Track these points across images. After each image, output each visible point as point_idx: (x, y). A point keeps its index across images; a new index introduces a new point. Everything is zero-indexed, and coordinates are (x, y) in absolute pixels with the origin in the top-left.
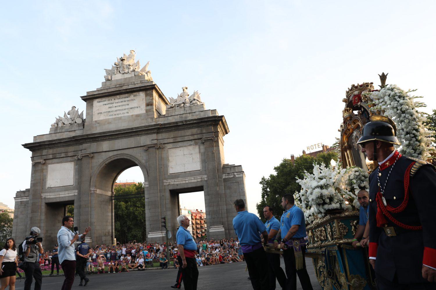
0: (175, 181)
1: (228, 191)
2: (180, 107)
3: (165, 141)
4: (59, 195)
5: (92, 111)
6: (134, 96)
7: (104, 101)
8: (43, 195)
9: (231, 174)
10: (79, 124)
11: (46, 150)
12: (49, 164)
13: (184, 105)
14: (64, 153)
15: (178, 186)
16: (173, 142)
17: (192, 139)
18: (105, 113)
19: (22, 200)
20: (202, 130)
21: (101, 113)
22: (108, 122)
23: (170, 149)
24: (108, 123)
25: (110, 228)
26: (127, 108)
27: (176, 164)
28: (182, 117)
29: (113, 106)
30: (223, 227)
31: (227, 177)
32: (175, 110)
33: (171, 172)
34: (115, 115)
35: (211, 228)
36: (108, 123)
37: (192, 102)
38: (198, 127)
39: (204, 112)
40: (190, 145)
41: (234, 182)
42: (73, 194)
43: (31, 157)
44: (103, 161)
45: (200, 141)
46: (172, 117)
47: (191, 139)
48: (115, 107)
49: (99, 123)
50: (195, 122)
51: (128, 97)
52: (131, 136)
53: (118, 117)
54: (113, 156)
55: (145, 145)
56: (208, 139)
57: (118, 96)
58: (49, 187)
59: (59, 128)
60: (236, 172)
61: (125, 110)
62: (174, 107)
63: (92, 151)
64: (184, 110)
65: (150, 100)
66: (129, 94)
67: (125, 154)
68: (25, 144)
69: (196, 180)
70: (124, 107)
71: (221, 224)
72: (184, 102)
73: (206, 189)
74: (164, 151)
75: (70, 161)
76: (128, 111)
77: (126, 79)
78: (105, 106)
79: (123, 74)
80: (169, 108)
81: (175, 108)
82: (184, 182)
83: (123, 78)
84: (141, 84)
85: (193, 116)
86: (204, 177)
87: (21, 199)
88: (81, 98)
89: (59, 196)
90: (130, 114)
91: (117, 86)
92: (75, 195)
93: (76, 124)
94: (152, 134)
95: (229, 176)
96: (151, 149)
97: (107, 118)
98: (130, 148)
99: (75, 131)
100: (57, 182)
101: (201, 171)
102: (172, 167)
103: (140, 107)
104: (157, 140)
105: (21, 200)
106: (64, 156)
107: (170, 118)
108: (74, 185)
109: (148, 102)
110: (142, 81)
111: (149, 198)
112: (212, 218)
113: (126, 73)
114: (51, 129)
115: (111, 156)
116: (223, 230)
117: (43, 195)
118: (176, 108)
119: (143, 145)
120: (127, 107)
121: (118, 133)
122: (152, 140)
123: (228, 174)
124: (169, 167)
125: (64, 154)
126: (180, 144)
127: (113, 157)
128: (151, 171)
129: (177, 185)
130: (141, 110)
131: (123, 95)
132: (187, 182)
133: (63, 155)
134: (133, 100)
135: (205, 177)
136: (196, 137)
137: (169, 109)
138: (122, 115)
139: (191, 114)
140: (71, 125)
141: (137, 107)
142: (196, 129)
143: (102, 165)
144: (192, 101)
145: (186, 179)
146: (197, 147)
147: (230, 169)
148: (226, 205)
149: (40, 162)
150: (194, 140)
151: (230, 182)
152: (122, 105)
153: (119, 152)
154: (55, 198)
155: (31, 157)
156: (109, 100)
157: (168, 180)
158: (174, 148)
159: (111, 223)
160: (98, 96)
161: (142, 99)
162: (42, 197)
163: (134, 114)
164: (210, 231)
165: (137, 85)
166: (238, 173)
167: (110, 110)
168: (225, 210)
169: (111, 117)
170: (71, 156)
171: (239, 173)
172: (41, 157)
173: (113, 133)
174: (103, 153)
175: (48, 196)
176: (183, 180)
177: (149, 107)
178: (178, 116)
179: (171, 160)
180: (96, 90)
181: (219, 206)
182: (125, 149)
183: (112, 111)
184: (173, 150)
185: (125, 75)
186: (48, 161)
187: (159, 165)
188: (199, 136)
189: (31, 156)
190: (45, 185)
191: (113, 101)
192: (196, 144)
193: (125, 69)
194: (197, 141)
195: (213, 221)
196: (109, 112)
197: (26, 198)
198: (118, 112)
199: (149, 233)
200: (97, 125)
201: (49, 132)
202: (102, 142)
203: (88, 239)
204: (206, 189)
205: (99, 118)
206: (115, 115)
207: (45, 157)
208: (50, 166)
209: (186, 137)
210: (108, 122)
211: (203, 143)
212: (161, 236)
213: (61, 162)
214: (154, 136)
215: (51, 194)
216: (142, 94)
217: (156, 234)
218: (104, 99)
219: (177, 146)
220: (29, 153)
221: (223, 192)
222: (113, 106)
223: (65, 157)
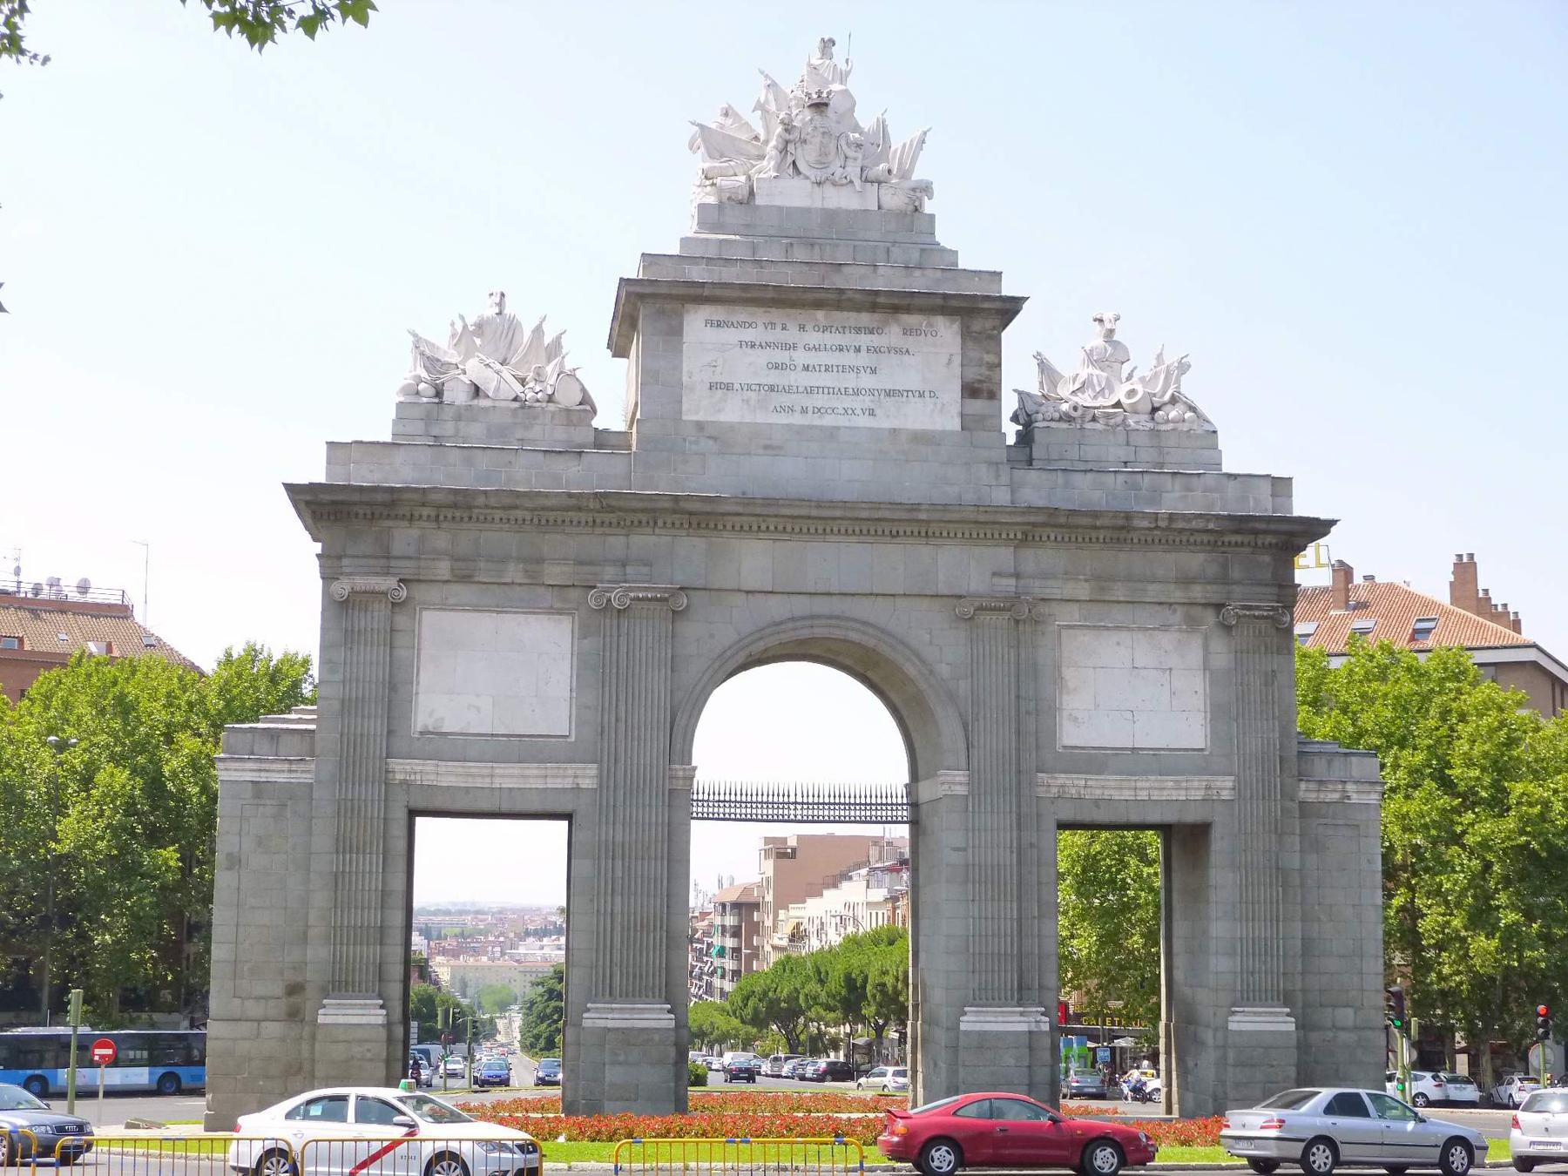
0: (1089, 783)
1: (1312, 859)
2: (1107, 425)
3: (1055, 591)
5: (678, 368)
6: (907, 331)
7: (742, 325)
8: (395, 764)
9: (1331, 787)
10: (568, 411)
11: (414, 533)
12: (428, 606)
14: (519, 560)
15: (1098, 806)
19: (263, 774)
20: (1225, 566)
21: (728, 387)
23: (1070, 631)
24: (766, 447)
26: (868, 386)
27: (1097, 706)
28: (1136, 487)
30: (1288, 1015)
31: (1311, 797)
33: (1068, 742)
35: (1234, 1013)
38: (1213, 546)
39: (1239, 479)
40: (1165, 627)
41: (1341, 822)
42: (568, 783)
44: (740, 641)
45: (1210, 617)
46: (1089, 475)
48: (806, 368)
49: (715, 438)
50: (1211, 526)
51: (871, 332)
53: (822, 428)
54: (793, 619)
55: (957, 591)
56: (1257, 613)
57: (820, 314)
58: (431, 729)
59: (448, 413)
60: (1356, 782)
61: (854, 397)
63: (681, 578)
64: (1128, 444)
65: (984, 371)
66: (877, 316)
67: (856, 620)
68: (311, 484)
69: (1183, 792)
70: (850, 381)
71: (1279, 999)
73: (1222, 838)
74: (1043, 634)
75: (551, 607)
77: (831, 217)
78: (749, 351)
79: (819, 184)
80: (1052, 420)
81: (1083, 422)
82: (1127, 795)
83: (818, 204)
84: (939, 274)
85: (1189, 489)
86: (1219, 784)
87: (260, 770)
89: (488, 780)
90: (883, 422)
91: (800, 254)
92: (577, 789)
93: (552, 407)
95: (1322, 796)
96: (986, 618)
97: (761, 418)
100: (478, 710)
101: (1207, 753)
102: (1076, 718)
103: (933, 394)
104: (1017, 576)
105: (257, 774)
107: (1083, 482)
109: (973, 374)
111: (965, 849)
112: (1242, 972)
113: (834, 184)
114: (400, 405)
115: (777, 619)
116: (1292, 1027)
117: (397, 768)
118: (1089, 426)
119: (943, 590)
120: (867, 381)
123: (1321, 782)
124: (1061, 717)
126: (1120, 614)
127: (790, 625)
128: (981, 721)
129: (1097, 802)
130: (941, 411)
132: (1143, 795)
133: (513, 572)
134: (898, 351)
135: (1225, 786)
136: (1197, 592)
137: (1053, 424)
138: (842, 421)
139: (1179, 481)
140: (522, 407)
142: (1202, 556)
143: (732, 656)
144: (1165, 404)
145: (1139, 784)
146: (1196, 642)
147: (1329, 763)
148: (1303, 921)
149: (385, 594)
150: (1185, 608)
153: (821, 606)
154: (467, 789)
155: (318, 555)
156: (773, 325)
157: (1056, 775)
158: (1089, 626)
160: (718, 292)
161: (945, 360)
162: (391, 776)
163: (902, 427)
164: (1232, 1026)
165: (917, 273)
166: (1361, 788)
167: (773, 378)
168: (1299, 943)
169: (783, 419)
171: (1367, 787)
172: (383, 562)
173: (814, 513)
174: (740, 599)
176: (1125, 784)
177: (977, 406)
178: (1121, 478)
179: (1071, 685)
180: (674, 249)
181: (1278, 921)
183: (787, 390)
184: (1085, 638)
185: (829, 190)
186: (420, 592)
187: (1018, 697)
188: (1214, 593)
190: (407, 717)
191: (792, 335)
192: (1192, 624)
193: (831, 158)
194: (1196, 611)
195: (1248, 985)
196: (772, 388)
197: (286, 766)
198: (819, 400)
199: (966, 1009)
201: (395, 423)
204: (1222, 838)
205: (719, 411)
206: (804, 411)
207: (407, 568)
208: (428, 617)
209: (1151, 587)
210: (768, 442)
211: (1227, 629)
212: (1024, 1028)
213: (499, 609)
214: (1004, 556)
215: (429, 766)
216: (947, 332)
217: (1000, 1019)
218: (741, 314)
219: (1101, 621)
221: (1297, 865)
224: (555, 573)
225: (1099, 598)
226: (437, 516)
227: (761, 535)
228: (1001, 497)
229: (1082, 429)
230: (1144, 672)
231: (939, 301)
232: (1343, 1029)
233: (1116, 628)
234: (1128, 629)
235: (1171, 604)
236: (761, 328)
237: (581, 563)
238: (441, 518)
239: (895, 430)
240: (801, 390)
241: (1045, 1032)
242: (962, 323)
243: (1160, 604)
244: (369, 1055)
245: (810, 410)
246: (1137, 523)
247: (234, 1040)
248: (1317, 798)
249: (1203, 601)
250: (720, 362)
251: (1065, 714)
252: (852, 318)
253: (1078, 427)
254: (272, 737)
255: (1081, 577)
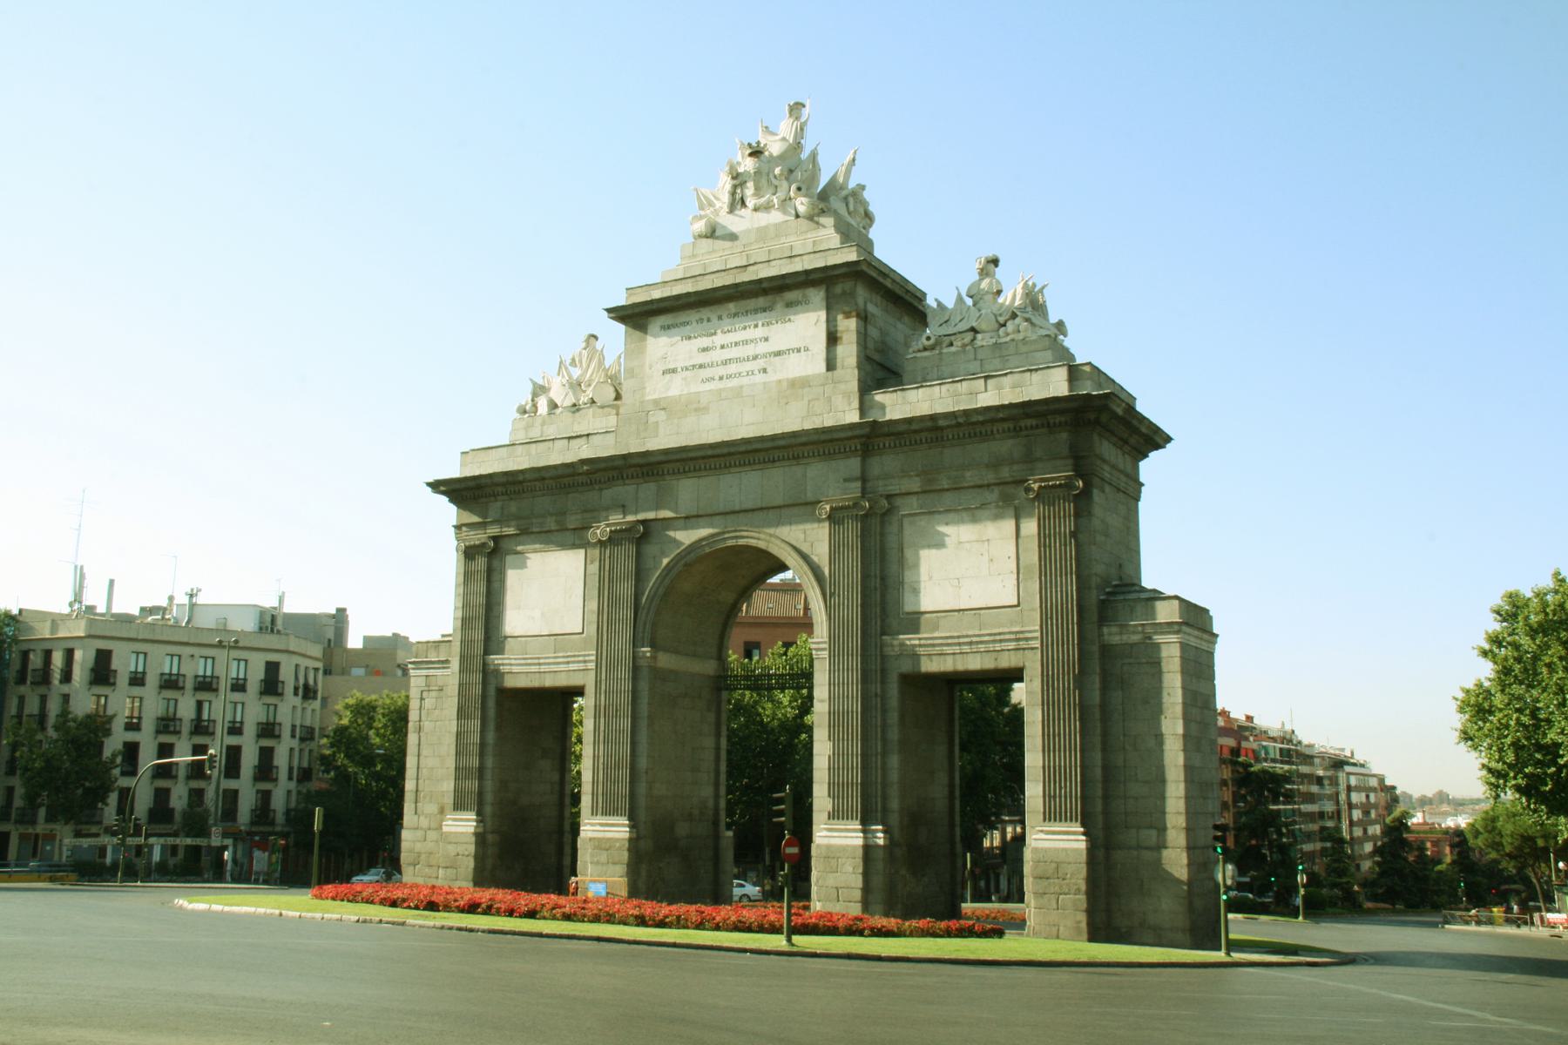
4: (539, 664)
11: (499, 504)
13: (974, 339)
14: (551, 515)
16: (919, 490)
17: (993, 481)
18: (687, 369)
21: (674, 371)
22: (694, 406)
23: (911, 519)
24: (696, 410)
25: (708, 791)
29: (713, 342)
31: (1116, 639)
32: (941, 359)
34: (721, 378)
36: (696, 410)
37: (1004, 325)
38: (1017, 431)
40: (983, 506)
41: (1144, 660)
43: (454, 526)
47: (986, 482)
48: (722, 347)
49: (664, 409)
50: (1001, 415)
51: (765, 311)
52: (774, 461)
57: (732, 306)
62: (938, 348)
64: (975, 359)
66: (770, 298)
70: (750, 350)
72: (974, 324)
76: (765, 366)
80: (919, 351)
81: (941, 348)
88: (606, 313)
90: (772, 377)
94: (848, 457)
95: (1125, 637)
98: (768, 508)
99: (588, 435)
103: (807, 349)
106: (553, 528)
108: (584, 635)
110: (821, 241)
118: (945, 350)
120: (762, 348)
121: (725, 451)
122: (846, 480)
124: (903, 588)
125: (554, 518)
126: (948, 498)
131: (748, 301)
133: (551, 523)
136: (1006, 473)
137: (919, 355)
138: (745, 381)
141: (799, 351)
142: (1011, 442)
150: (1001, 487)
151: (1126, 661)
152: (746, 342)
155: (454, 526)
156: (702, 320)
159: (712, 775)
170: (575, 529)
175: (505, 667)
182: (753, 510)
183: (711, 365)
189: (455, 523)
194: (1010, 490)
196: (701, 366)
198: (733, 369)
200: (662, 416)
202: (675, 482)
203: (623, 825)
209: (968, 474)
220: (447, 512)
222: (713, 342)
223: (557, 531)
224: (573, 521)
225: (928, 488)
226: (506, 491)
227: (690, 475)
228: (853, 417)
229: (941, 353)
230: (967, 545)
231: (802, 278)
232: (1147, 848)
233: (947, 511)
234: (956, 511)
235: (988, 486)
236: (694, 324)
237: (585, 511)
238: (509, 492)
239: (780, 381)
240: (719, 363)
241: (880, 846)
242: (827, 291)
243: (980, 486)
244: (466, 853)
245: (725, 377)
246: (941, 423)
247: (414, 842)
248: (1121, 640)
249: (1010, 479)
250: (669, 354)
251: (906, 586)
252: (752, 303)
253: (937, 352)
254: (436, 647)
255: (912, 473)
